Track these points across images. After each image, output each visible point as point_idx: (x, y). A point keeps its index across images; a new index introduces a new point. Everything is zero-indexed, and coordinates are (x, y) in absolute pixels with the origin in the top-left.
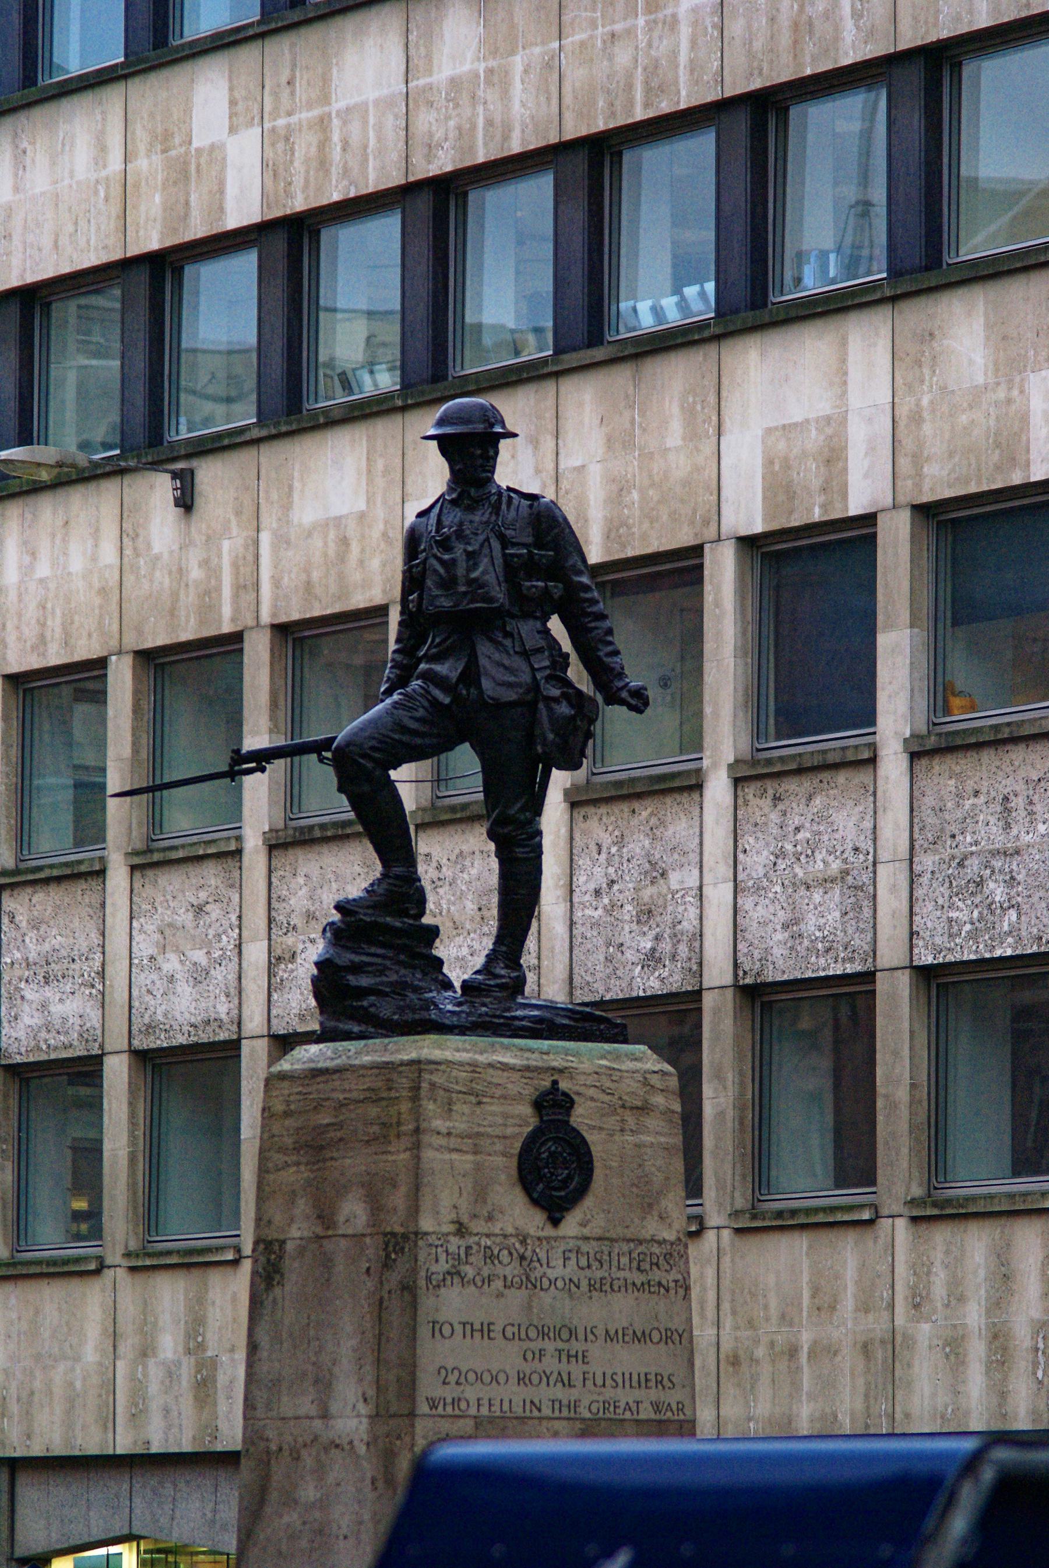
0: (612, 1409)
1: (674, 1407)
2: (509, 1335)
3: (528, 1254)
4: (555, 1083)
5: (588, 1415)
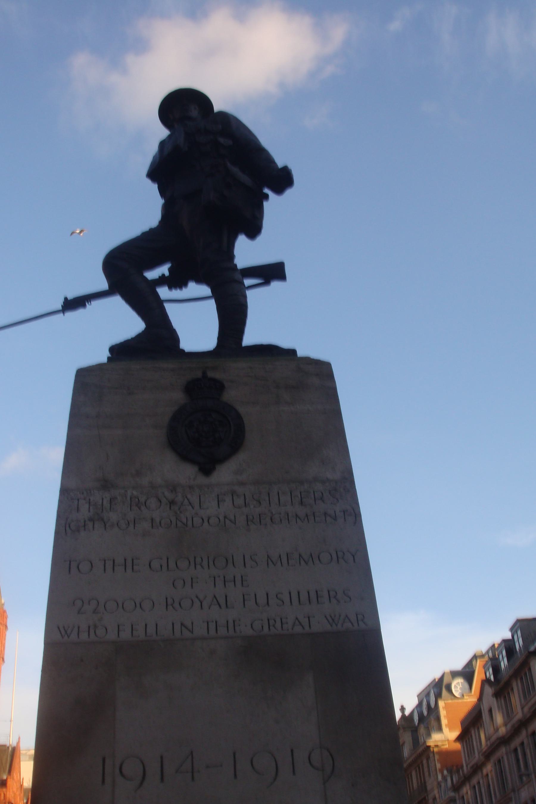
0: (278, 625)
1: (353, 618)
2: (155, 564)
3: (179, 498)
4: (204, 374)
5: (250, 632)
